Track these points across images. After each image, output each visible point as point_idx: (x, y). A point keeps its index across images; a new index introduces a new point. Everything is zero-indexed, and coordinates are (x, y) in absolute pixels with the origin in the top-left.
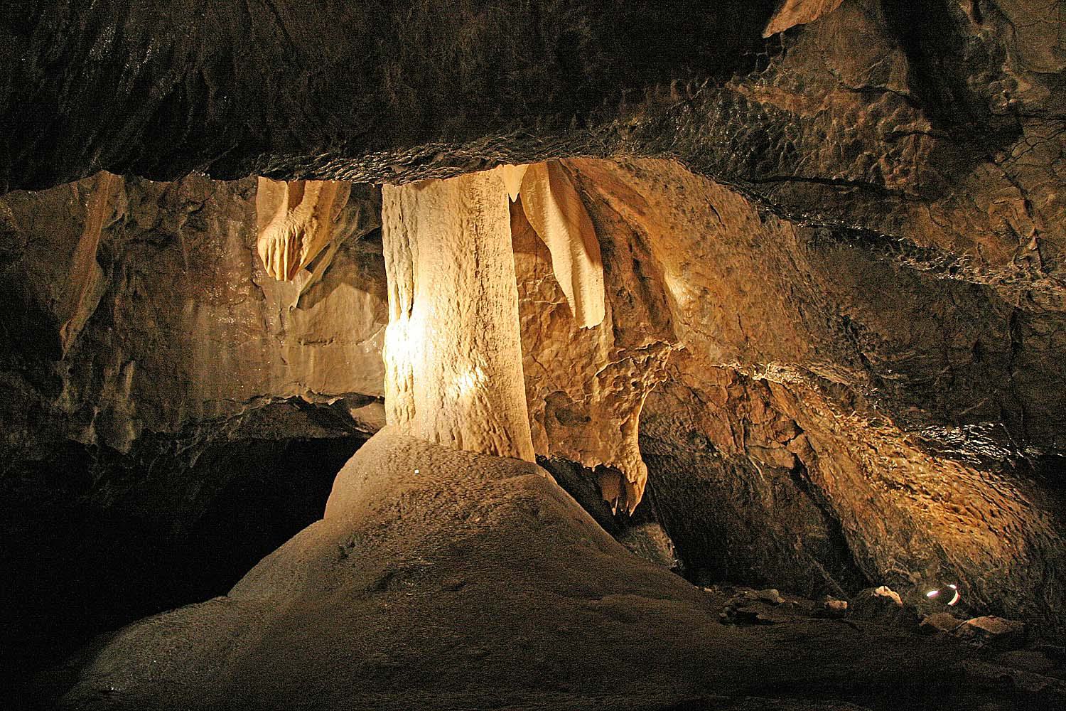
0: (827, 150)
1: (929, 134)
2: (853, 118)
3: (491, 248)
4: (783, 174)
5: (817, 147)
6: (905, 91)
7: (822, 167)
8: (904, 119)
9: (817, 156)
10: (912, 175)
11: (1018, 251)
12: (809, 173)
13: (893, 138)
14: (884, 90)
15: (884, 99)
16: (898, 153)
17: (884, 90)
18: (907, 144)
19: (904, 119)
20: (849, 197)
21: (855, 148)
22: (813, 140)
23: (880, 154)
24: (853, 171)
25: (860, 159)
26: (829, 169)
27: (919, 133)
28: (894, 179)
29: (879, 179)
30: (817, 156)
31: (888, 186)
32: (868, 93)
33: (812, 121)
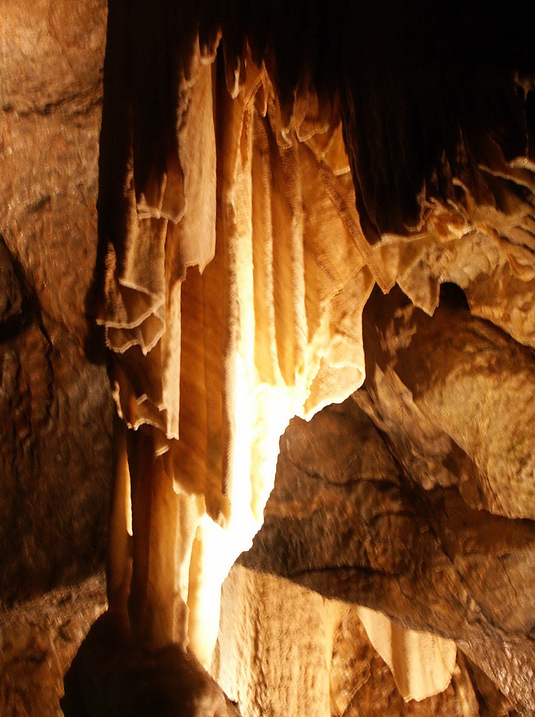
0: (329, 540)
1: (399, 514)
2: (343, 510)
3: (275, 631)
4: (303, 567)
5: (319, 541)
6: (380, 476)
7: (327, 557)
8: (377, 503)
9: (321, 547)
10: (389, 552)
11: (466, 615)
12: (317, 563)
13: (373, 521)
14: (359, 481)
15: (360, 488)
16: (378, 534)
17: (359, 481)
18: (383, 523)
19: (377, 503)
20: (347, 581)
21: (347, 536)
22: (316, 534)
23: (364, 537)
24: (347, 558)
25: (352, 545)
26: (333, 557)
27: (389, 513)
28: (376, 559)
29: (368, 561)
30: (321, 547)
31: (373, 565)
32: (350, 485)
33: (311, 519)
